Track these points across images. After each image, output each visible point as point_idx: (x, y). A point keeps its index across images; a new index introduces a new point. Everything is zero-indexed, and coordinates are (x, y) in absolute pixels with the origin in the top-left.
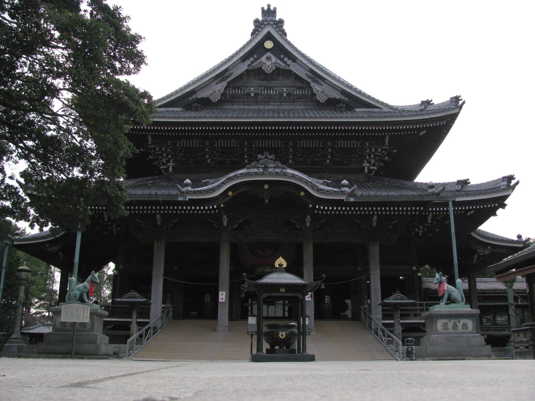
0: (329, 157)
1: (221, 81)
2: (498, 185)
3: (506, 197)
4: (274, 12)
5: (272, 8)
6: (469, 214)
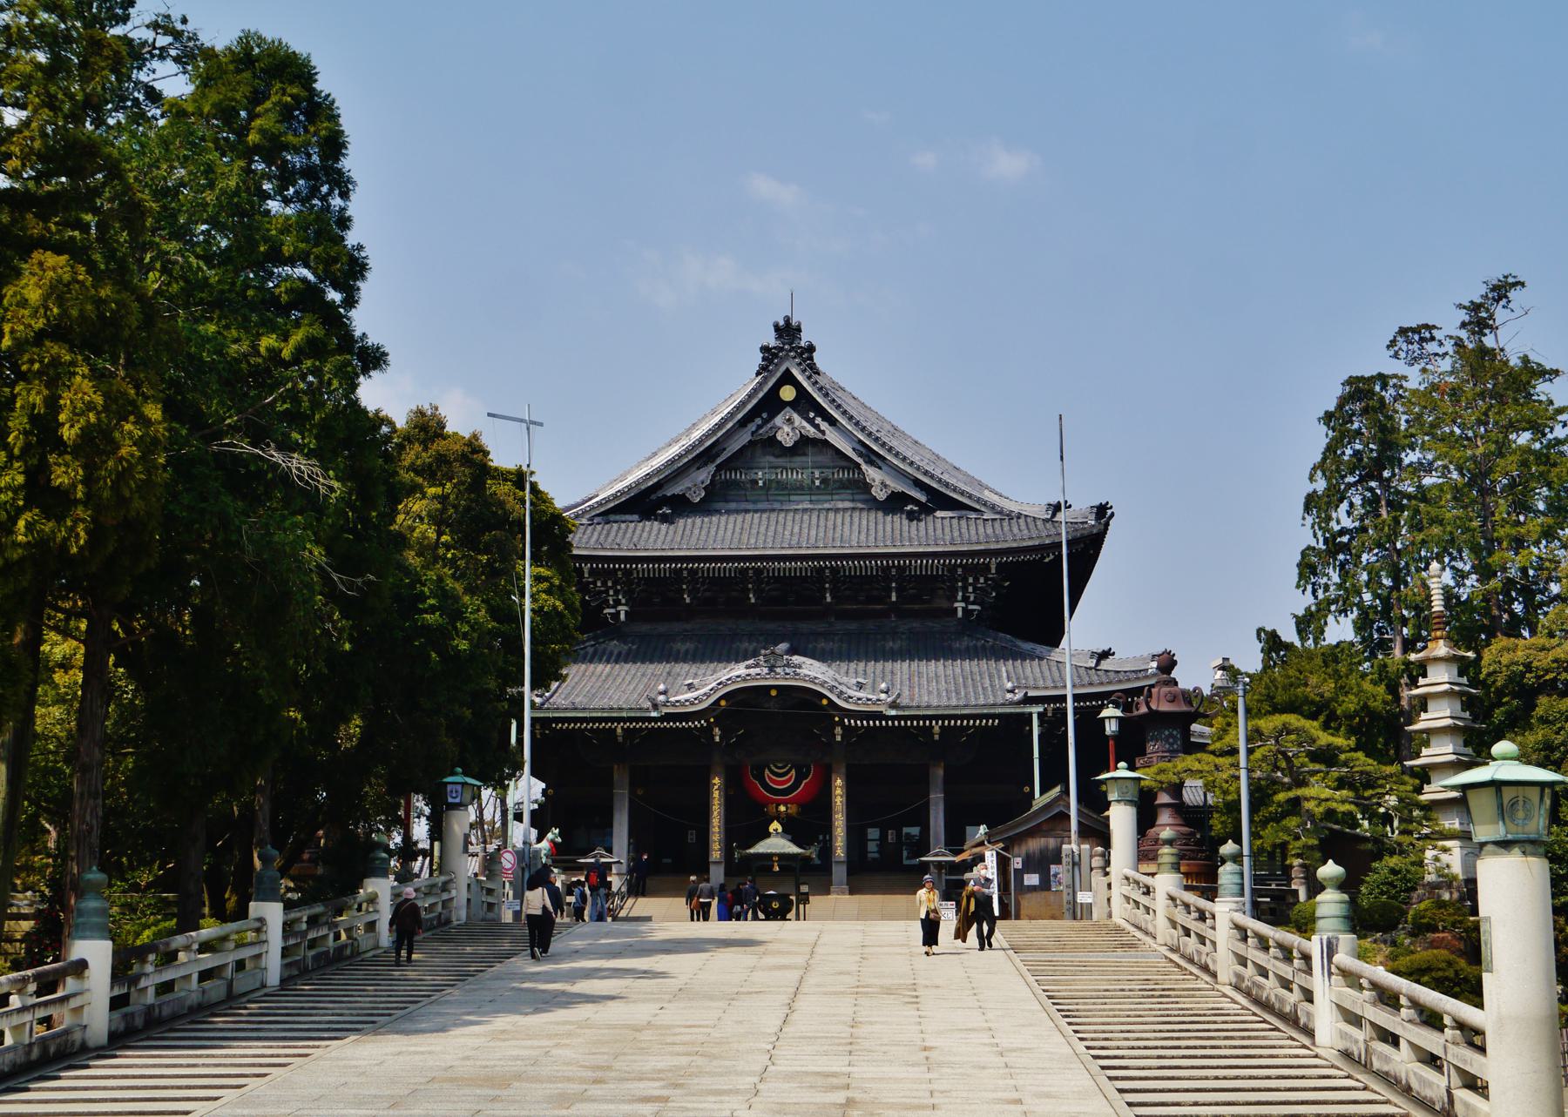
1: (706, 464)
5: (794, 322)
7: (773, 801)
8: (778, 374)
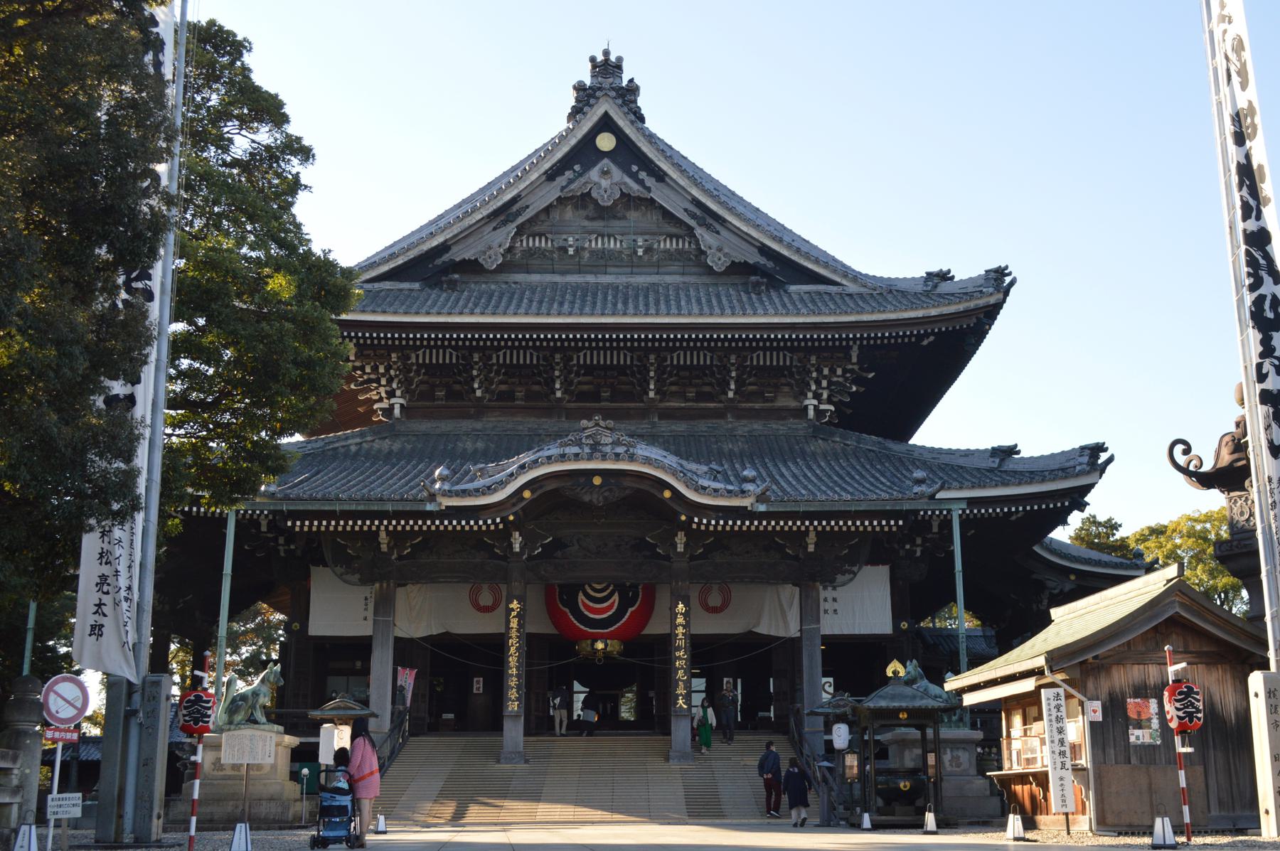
0: (733, 387)
1: (504, 223)
2: (1072, 463)
3: (1089, 487)
4: (618, 67)
5: (613, 58)
6: (1014, 518)
7: (586, 636)
8: (595, 119)
